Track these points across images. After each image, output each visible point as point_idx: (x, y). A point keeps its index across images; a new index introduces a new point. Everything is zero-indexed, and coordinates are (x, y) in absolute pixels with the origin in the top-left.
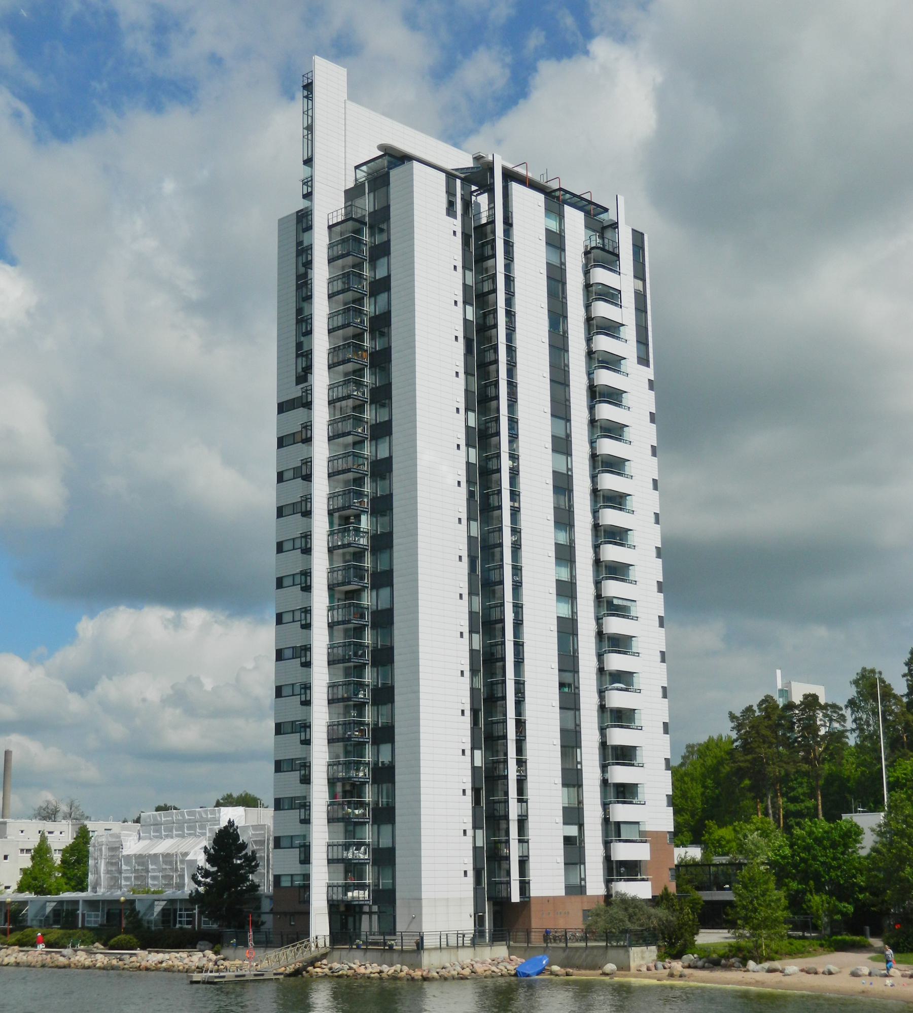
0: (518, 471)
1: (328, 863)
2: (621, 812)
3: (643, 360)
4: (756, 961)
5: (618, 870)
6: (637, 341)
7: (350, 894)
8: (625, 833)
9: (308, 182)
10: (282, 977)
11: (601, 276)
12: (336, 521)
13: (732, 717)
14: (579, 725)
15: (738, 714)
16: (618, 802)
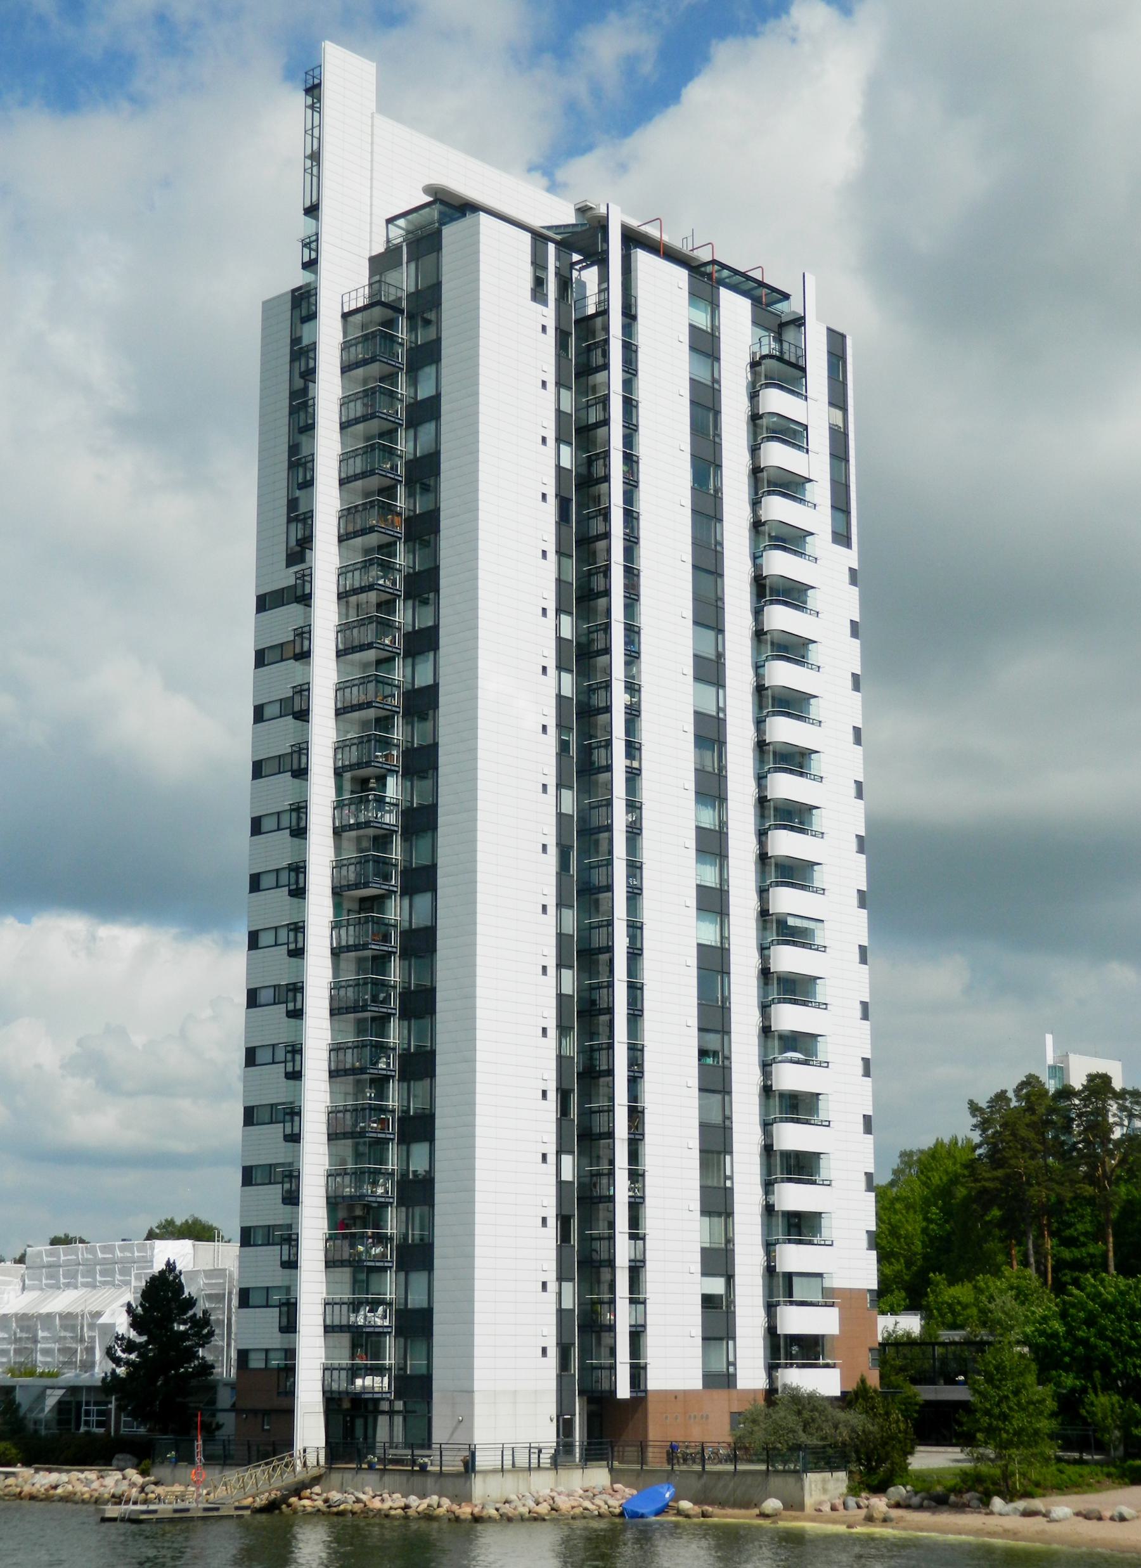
0: (639, 711)
1: (326, 1332)
2: (794, 1257)
3: (842, 538)
4: (1004, 1498)
5: (784, 1349)
6: (833, 507)
7: (359, 1382)
9: (311, 243)
10: (247, 1513)
11: (776, 401)
12: (347, 786)
13: (974, 1108)
14: (730, 1118)
15: (983, 1104)
16: (790, 1241)
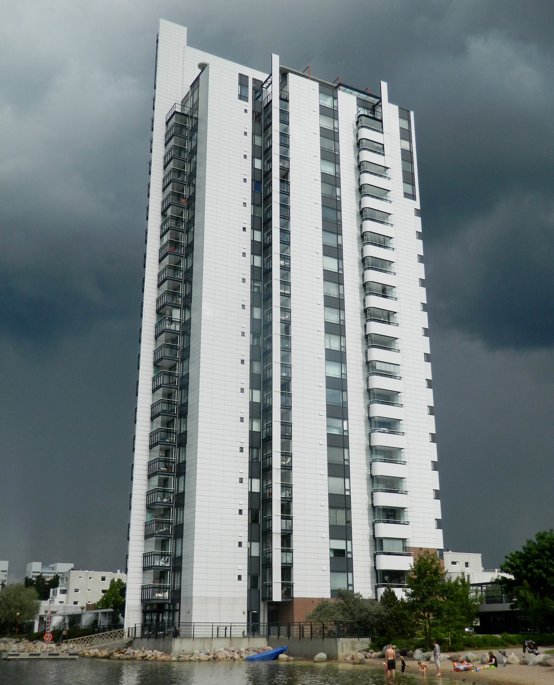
2: (385, 530)
3: (411, 196)
11: (365, 133)
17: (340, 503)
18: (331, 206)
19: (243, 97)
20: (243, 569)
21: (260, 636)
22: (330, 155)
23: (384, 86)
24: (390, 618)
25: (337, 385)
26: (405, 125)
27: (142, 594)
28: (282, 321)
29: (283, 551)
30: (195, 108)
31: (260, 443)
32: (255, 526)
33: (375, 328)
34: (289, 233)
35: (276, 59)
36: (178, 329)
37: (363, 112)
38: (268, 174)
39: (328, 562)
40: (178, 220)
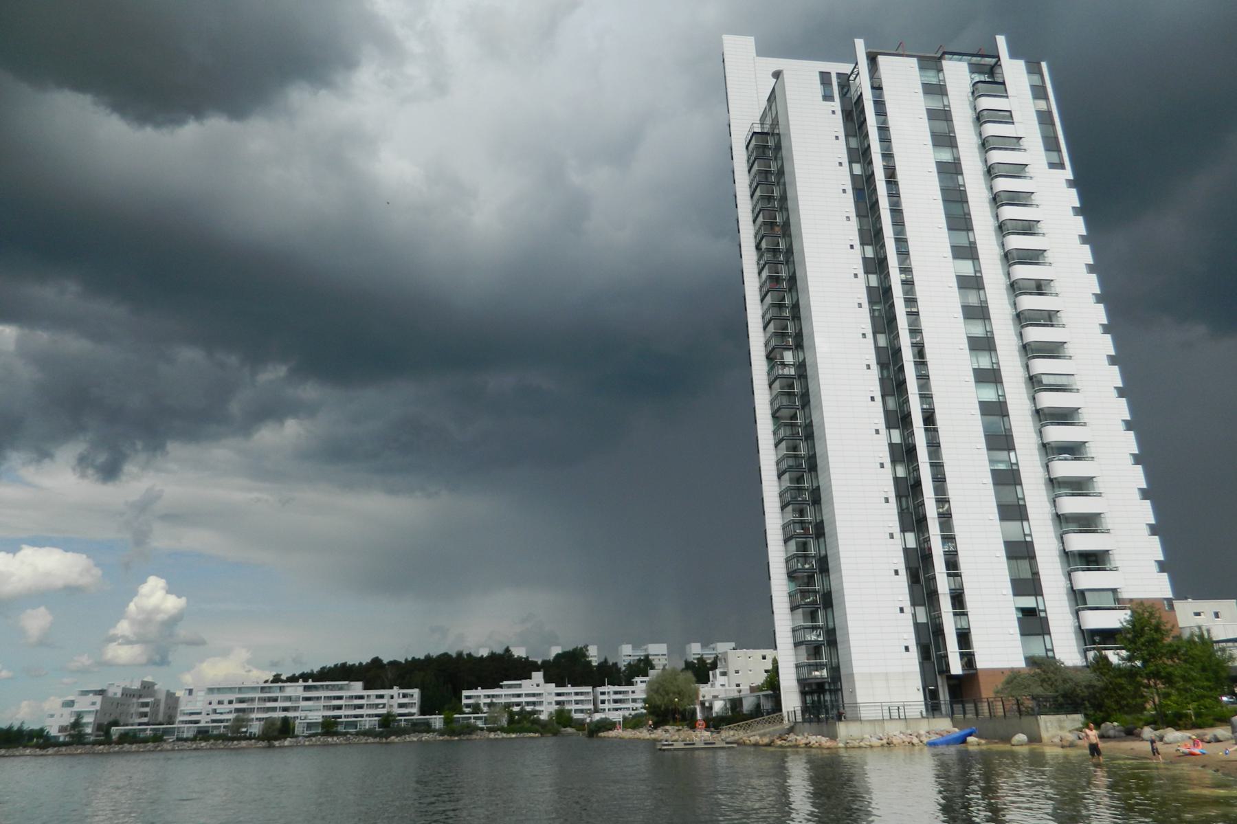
2: (1086, 579)
8: (1091, 600)
11: (986, 103)
17: (1020, 551)
18: (955, 199)
19: (828, 97)
20: (910, 639)
21: (942, 716)
22: (944, 138)
23: (1001, 41)
24: (1106, 688)
25: (995, 411)
26: (1038, 82)
27: (798, 673)
28: (914, 345)
29: (955, 614)
30: (775, 123)
31: (908, 490)
32: (916, 587)
33: (1035, 334)
34: (905, 241)
35: (860, 45)
36: (793, 372)
37: (977, 78)
38: (870, 178)
39: (1016, 624)
40: (775, 251)
